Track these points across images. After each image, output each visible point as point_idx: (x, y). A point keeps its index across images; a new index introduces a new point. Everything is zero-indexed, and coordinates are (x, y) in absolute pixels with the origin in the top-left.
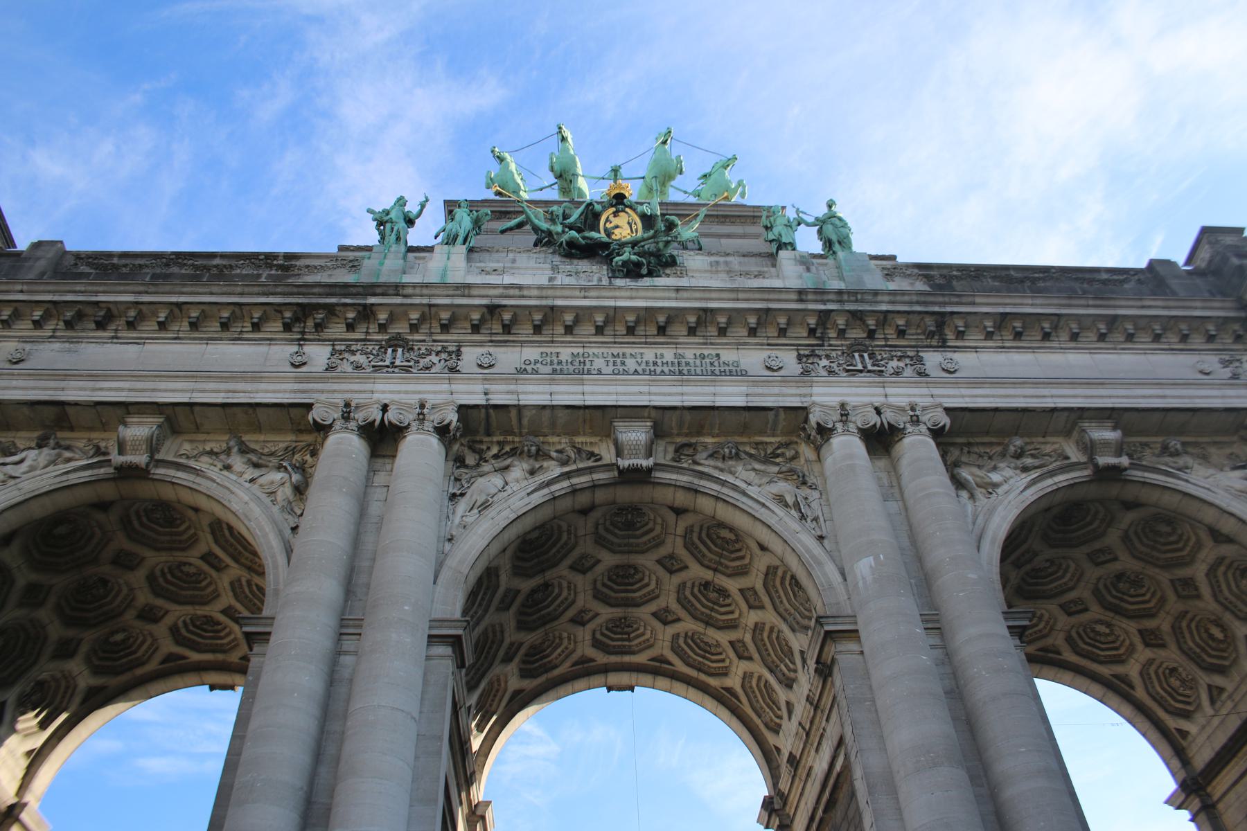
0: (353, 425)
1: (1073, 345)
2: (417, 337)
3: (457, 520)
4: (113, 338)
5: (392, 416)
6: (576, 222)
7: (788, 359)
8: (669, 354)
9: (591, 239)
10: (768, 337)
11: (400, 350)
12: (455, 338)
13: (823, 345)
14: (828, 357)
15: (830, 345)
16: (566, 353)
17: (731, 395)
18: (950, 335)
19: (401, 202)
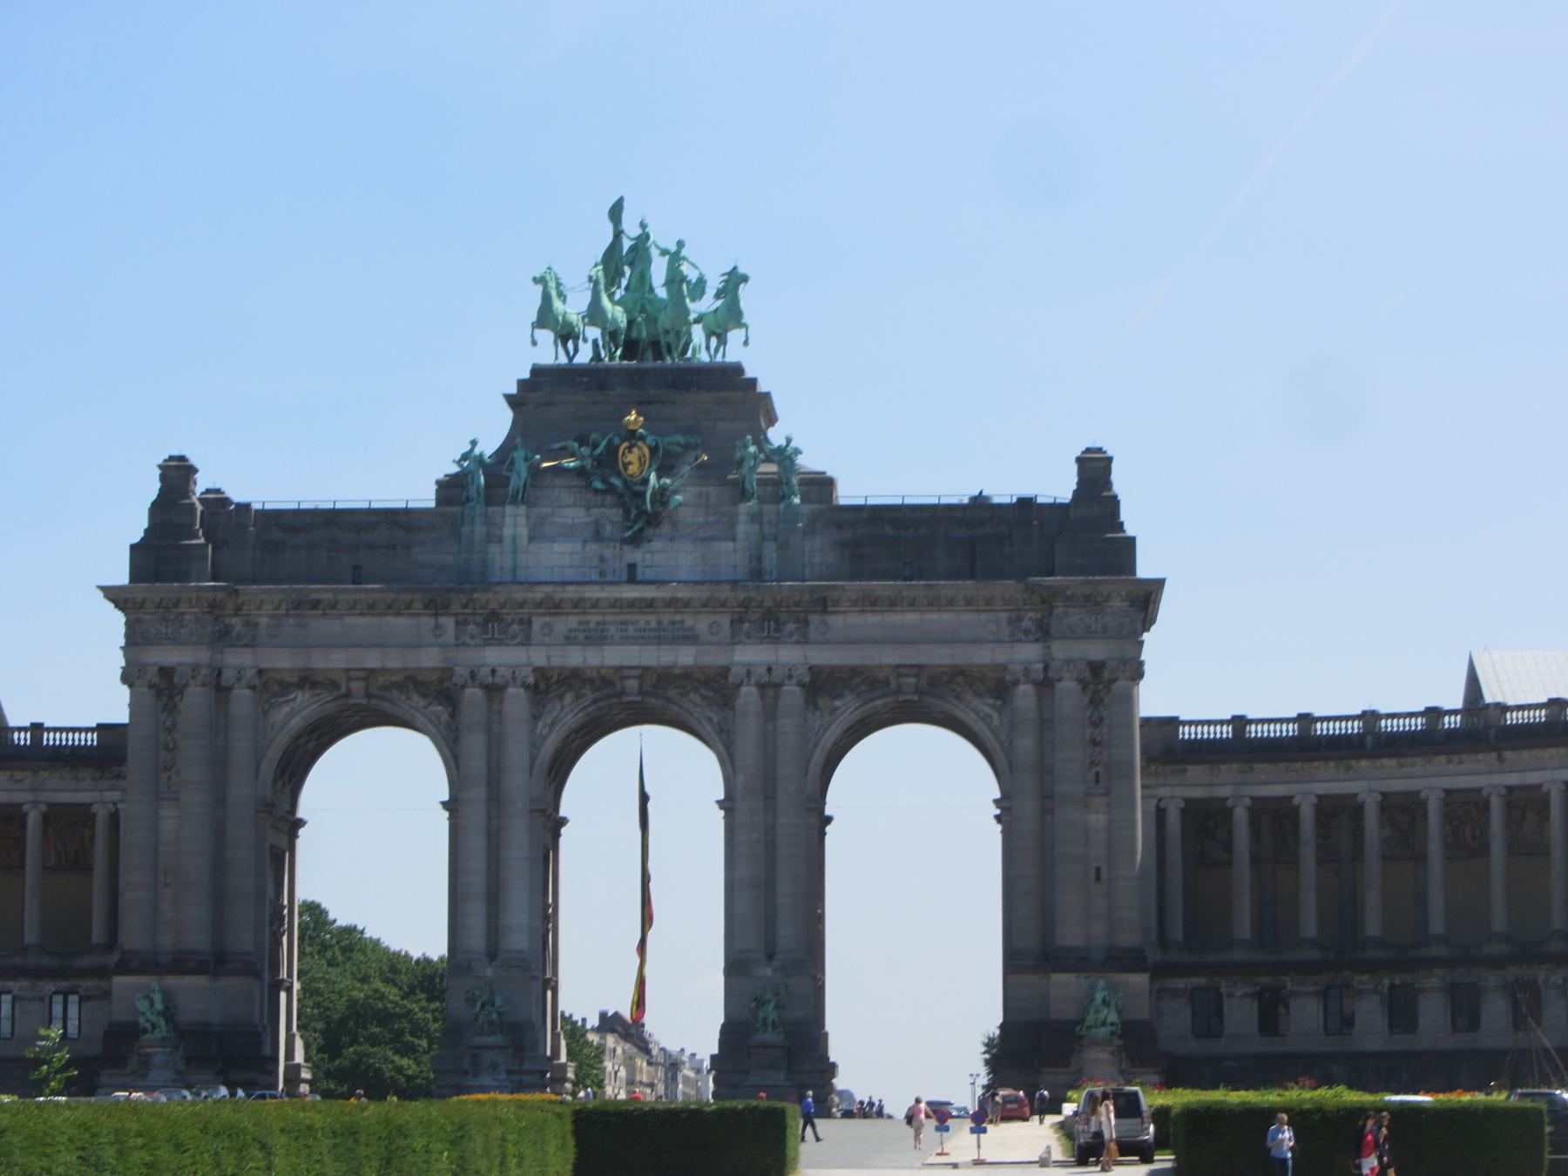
0: (477, 683)
1: (910, 608)
2: (505, 611)
3: (538, 733)
4: (324, 615)
5: (498, 680)
6: (600, 454)
7: (725, 621)
8: (653, 620)
9: (612, 485)
10: (714, 607)
11: (496, 625)
12: (526, 611)
13: (747, 612)
14: (750, 621)
15: (753, 612)
16: (594, 619)
17: (685, 656)
18: (830, 604)
19: (474, 443)
